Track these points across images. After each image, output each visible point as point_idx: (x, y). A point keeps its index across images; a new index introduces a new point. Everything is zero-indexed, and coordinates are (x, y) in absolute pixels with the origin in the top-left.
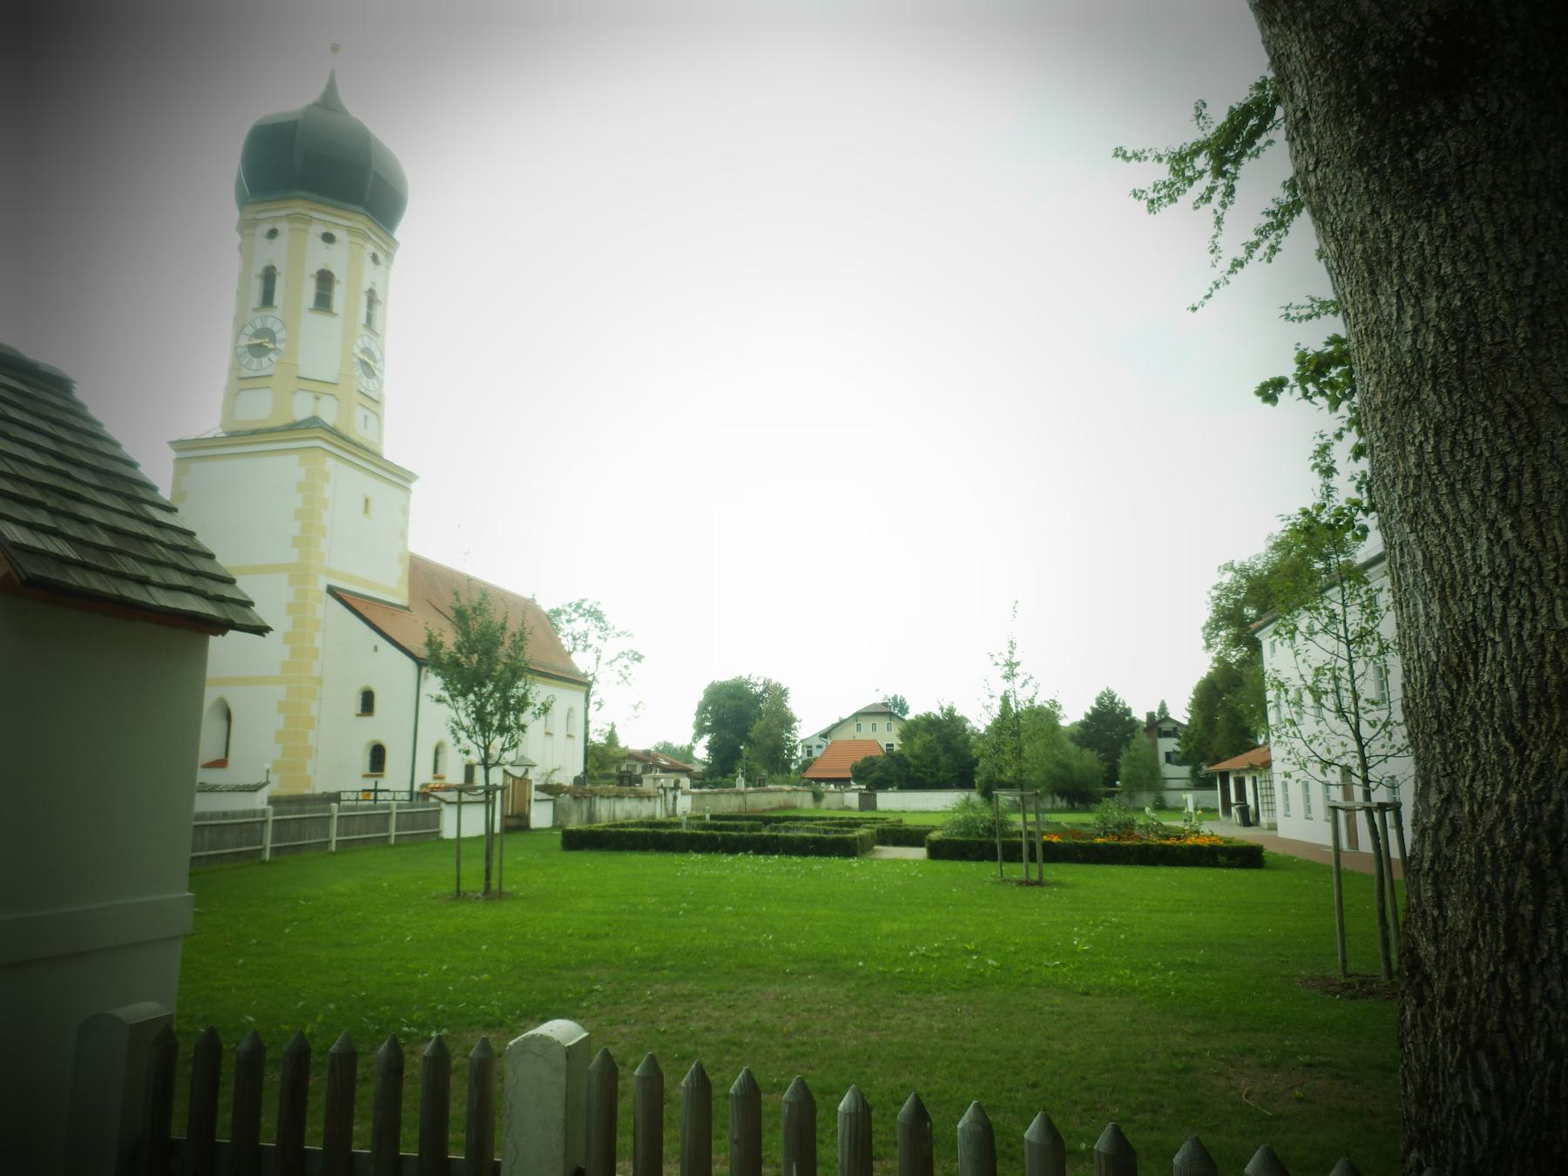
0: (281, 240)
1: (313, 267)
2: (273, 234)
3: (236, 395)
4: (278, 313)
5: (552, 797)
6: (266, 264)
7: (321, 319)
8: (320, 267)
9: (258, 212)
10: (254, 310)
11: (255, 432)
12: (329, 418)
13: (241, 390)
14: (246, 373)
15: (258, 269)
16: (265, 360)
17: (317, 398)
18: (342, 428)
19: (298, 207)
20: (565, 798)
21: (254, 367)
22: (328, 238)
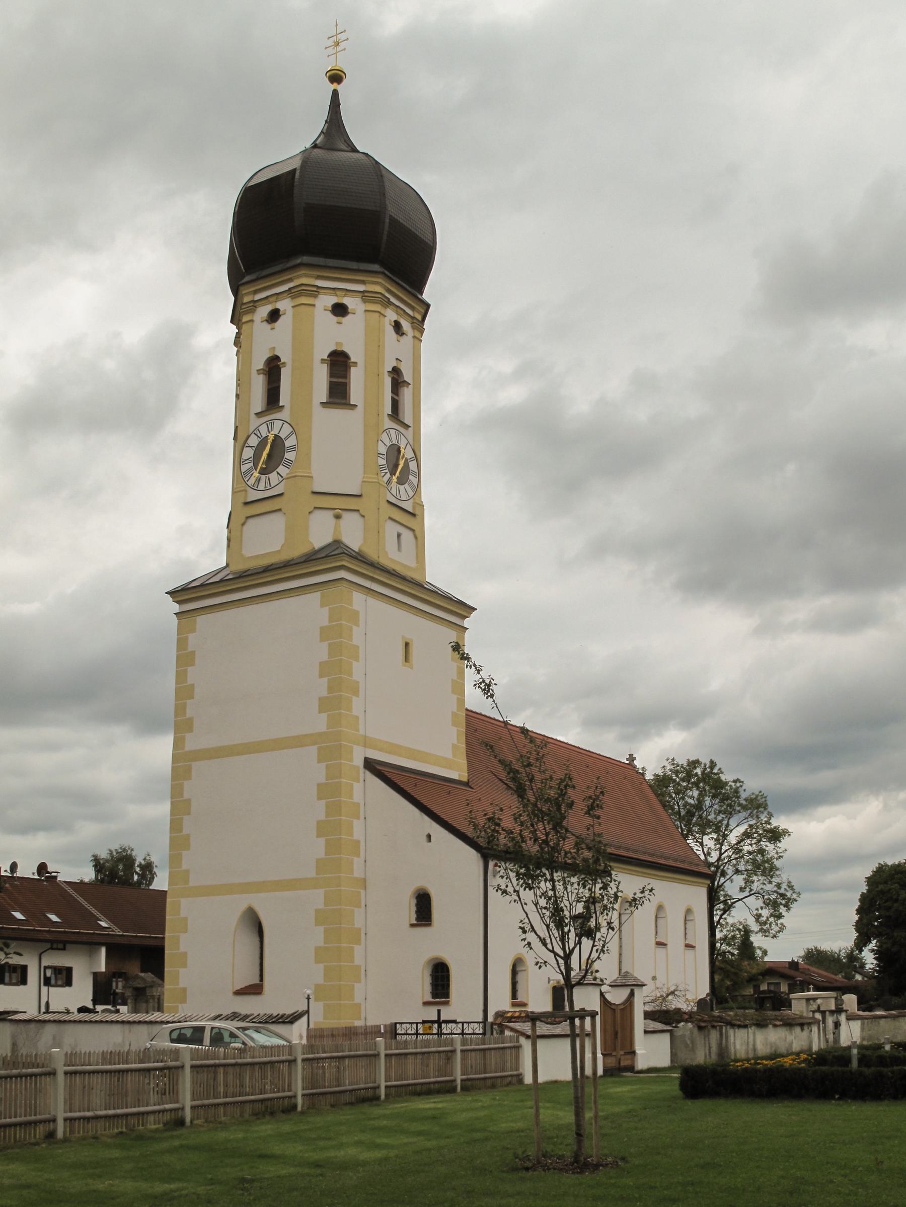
0: (284, 322)
1: (323, 351)
2: (274, 316)
3: (243, 524)
4: (285, 414)
5: (669, 1028)
6: (267, 355)
7: (338, 414)
9: (256, 292)
10: (258, 415)
12: (354, 540)
13: (247, 518)
14: (253, 495)
15: (259, 362)
17: (338, 517)
18: (372, 554)
19: (304, 279)
20: (685, 1028)
21: (261, 487)
22: (340, 310)
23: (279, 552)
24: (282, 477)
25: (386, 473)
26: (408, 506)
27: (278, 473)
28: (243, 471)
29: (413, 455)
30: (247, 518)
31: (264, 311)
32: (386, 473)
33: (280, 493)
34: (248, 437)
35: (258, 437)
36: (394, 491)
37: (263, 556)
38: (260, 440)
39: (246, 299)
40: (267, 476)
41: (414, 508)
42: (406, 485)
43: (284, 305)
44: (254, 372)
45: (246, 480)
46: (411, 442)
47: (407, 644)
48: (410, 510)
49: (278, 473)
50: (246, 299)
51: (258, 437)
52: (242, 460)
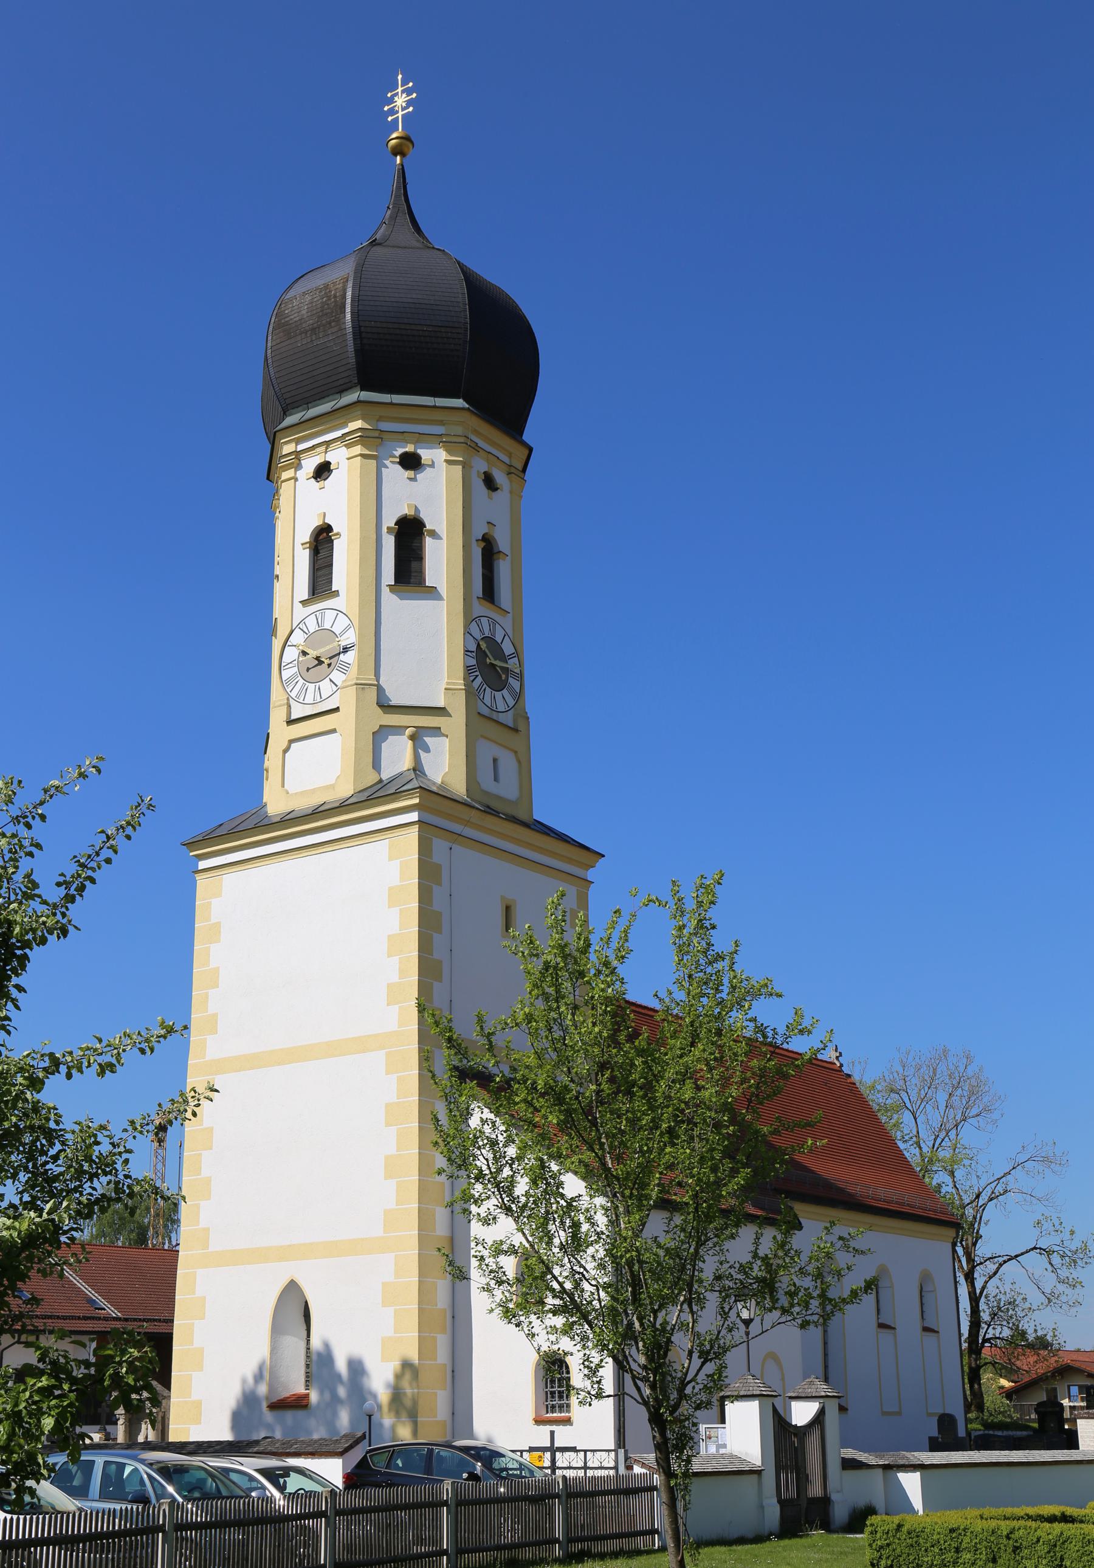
2: (323, 471)
3: (285, 751)
6: (317, 522)
8: (406, 511)
9: (298, 441)
11: (317, 813)
13: (291, 742)
16: (326, 687)
21: (309, 699)
23: (332, 787)
24: (337, 686)
25: (477, 676)
26: (508, 719)
27: (331, 680)
28: (284, 679)
29: (514, 651)
30: (291, 742)
31: (310, 464)
32: (477, 676)
33: (335, 707)
34: (292, 632)
35: (304, 632)
36: (487, 700)
37: (313, 791)
38: (306, 636)
39: (287, 449)
40: (317, 684)
41: (515, 720)
42: (505, 692)
43: (338, 456)
44: (298, 547)
45: (288, 690)
46: (510, 633)
47: (508, 908)
48: (511, 724)
49: (331, 680)
50: (287, 449)
51: (304, 632)
52: (283, 664)
